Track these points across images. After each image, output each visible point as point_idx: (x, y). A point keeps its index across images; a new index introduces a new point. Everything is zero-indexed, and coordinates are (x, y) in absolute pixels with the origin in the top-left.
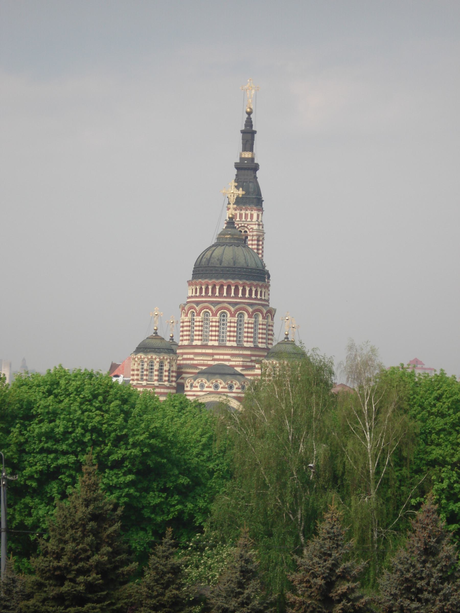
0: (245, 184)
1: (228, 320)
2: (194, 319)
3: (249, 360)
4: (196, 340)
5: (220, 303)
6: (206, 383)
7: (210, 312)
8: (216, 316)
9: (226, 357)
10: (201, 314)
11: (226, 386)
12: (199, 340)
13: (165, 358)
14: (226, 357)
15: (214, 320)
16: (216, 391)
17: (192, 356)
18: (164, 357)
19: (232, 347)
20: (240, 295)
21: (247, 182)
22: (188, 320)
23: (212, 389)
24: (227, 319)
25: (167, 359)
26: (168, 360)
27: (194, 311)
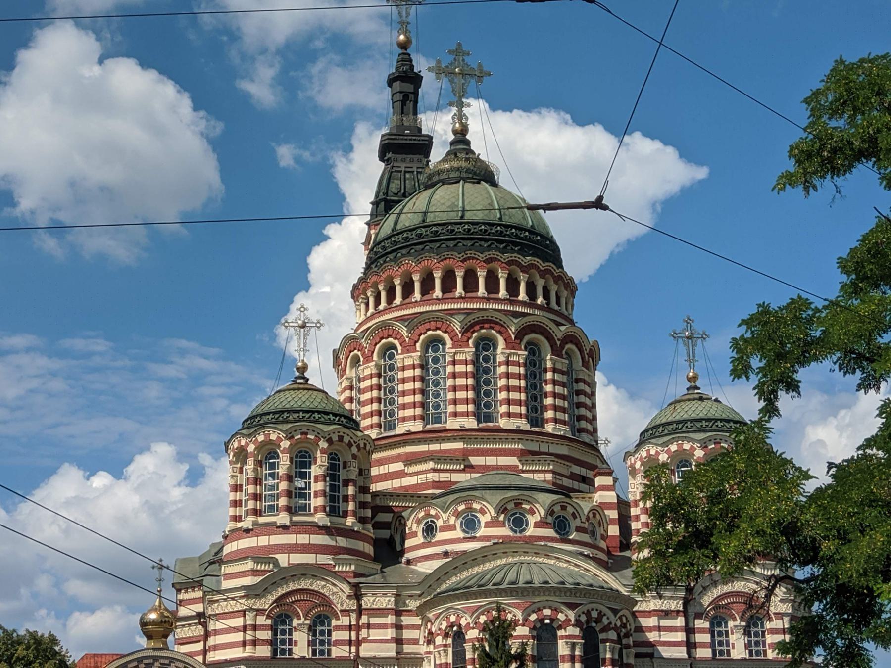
0: (407, 176)
1: (500, 358)
2: (392, 367)
3: (566, 472)
4: (404, 419)
5: (469, 312)
6: (482, 512)
7: (446, 337)
8: (468, 346)
9: (504, 461)
10: (418, 345)
11: (550, 519)
12: (414, 418)
13: (346, 440)
14: (504, 461)
15: (458, 357)
16: (518, 534)
17: (398, 466)
18: (341, 439)
19: (518, 431)
20: (522, 296)
21: (413, 172)
22: (374, 371)
23: (505, 531)
24: (495, 357)
25: (350, 445)
26: (354, 450)
27: (396, 342)
